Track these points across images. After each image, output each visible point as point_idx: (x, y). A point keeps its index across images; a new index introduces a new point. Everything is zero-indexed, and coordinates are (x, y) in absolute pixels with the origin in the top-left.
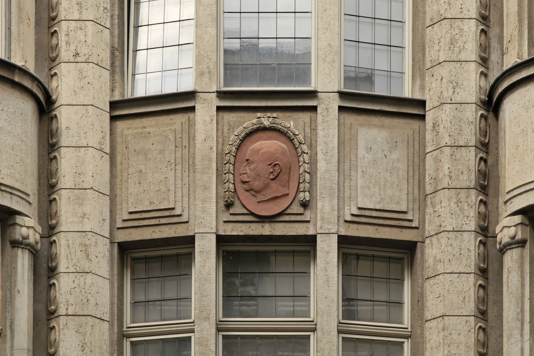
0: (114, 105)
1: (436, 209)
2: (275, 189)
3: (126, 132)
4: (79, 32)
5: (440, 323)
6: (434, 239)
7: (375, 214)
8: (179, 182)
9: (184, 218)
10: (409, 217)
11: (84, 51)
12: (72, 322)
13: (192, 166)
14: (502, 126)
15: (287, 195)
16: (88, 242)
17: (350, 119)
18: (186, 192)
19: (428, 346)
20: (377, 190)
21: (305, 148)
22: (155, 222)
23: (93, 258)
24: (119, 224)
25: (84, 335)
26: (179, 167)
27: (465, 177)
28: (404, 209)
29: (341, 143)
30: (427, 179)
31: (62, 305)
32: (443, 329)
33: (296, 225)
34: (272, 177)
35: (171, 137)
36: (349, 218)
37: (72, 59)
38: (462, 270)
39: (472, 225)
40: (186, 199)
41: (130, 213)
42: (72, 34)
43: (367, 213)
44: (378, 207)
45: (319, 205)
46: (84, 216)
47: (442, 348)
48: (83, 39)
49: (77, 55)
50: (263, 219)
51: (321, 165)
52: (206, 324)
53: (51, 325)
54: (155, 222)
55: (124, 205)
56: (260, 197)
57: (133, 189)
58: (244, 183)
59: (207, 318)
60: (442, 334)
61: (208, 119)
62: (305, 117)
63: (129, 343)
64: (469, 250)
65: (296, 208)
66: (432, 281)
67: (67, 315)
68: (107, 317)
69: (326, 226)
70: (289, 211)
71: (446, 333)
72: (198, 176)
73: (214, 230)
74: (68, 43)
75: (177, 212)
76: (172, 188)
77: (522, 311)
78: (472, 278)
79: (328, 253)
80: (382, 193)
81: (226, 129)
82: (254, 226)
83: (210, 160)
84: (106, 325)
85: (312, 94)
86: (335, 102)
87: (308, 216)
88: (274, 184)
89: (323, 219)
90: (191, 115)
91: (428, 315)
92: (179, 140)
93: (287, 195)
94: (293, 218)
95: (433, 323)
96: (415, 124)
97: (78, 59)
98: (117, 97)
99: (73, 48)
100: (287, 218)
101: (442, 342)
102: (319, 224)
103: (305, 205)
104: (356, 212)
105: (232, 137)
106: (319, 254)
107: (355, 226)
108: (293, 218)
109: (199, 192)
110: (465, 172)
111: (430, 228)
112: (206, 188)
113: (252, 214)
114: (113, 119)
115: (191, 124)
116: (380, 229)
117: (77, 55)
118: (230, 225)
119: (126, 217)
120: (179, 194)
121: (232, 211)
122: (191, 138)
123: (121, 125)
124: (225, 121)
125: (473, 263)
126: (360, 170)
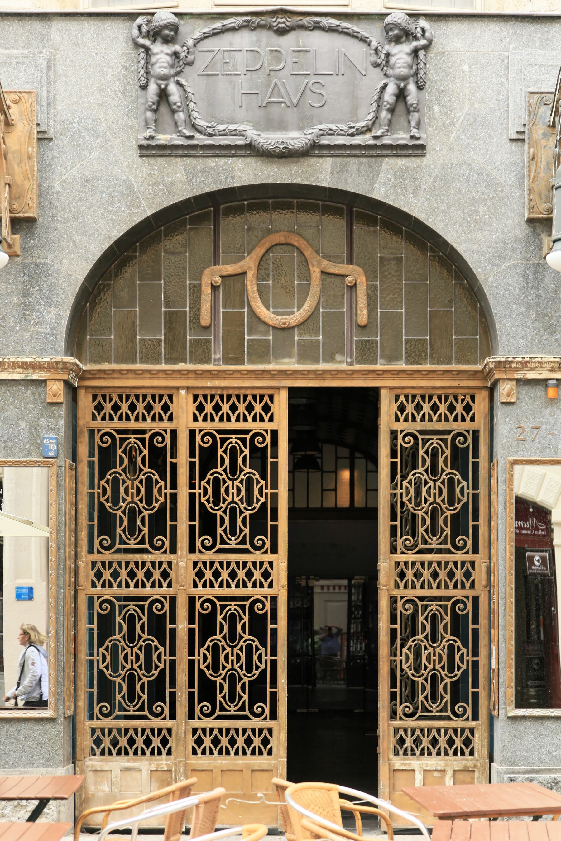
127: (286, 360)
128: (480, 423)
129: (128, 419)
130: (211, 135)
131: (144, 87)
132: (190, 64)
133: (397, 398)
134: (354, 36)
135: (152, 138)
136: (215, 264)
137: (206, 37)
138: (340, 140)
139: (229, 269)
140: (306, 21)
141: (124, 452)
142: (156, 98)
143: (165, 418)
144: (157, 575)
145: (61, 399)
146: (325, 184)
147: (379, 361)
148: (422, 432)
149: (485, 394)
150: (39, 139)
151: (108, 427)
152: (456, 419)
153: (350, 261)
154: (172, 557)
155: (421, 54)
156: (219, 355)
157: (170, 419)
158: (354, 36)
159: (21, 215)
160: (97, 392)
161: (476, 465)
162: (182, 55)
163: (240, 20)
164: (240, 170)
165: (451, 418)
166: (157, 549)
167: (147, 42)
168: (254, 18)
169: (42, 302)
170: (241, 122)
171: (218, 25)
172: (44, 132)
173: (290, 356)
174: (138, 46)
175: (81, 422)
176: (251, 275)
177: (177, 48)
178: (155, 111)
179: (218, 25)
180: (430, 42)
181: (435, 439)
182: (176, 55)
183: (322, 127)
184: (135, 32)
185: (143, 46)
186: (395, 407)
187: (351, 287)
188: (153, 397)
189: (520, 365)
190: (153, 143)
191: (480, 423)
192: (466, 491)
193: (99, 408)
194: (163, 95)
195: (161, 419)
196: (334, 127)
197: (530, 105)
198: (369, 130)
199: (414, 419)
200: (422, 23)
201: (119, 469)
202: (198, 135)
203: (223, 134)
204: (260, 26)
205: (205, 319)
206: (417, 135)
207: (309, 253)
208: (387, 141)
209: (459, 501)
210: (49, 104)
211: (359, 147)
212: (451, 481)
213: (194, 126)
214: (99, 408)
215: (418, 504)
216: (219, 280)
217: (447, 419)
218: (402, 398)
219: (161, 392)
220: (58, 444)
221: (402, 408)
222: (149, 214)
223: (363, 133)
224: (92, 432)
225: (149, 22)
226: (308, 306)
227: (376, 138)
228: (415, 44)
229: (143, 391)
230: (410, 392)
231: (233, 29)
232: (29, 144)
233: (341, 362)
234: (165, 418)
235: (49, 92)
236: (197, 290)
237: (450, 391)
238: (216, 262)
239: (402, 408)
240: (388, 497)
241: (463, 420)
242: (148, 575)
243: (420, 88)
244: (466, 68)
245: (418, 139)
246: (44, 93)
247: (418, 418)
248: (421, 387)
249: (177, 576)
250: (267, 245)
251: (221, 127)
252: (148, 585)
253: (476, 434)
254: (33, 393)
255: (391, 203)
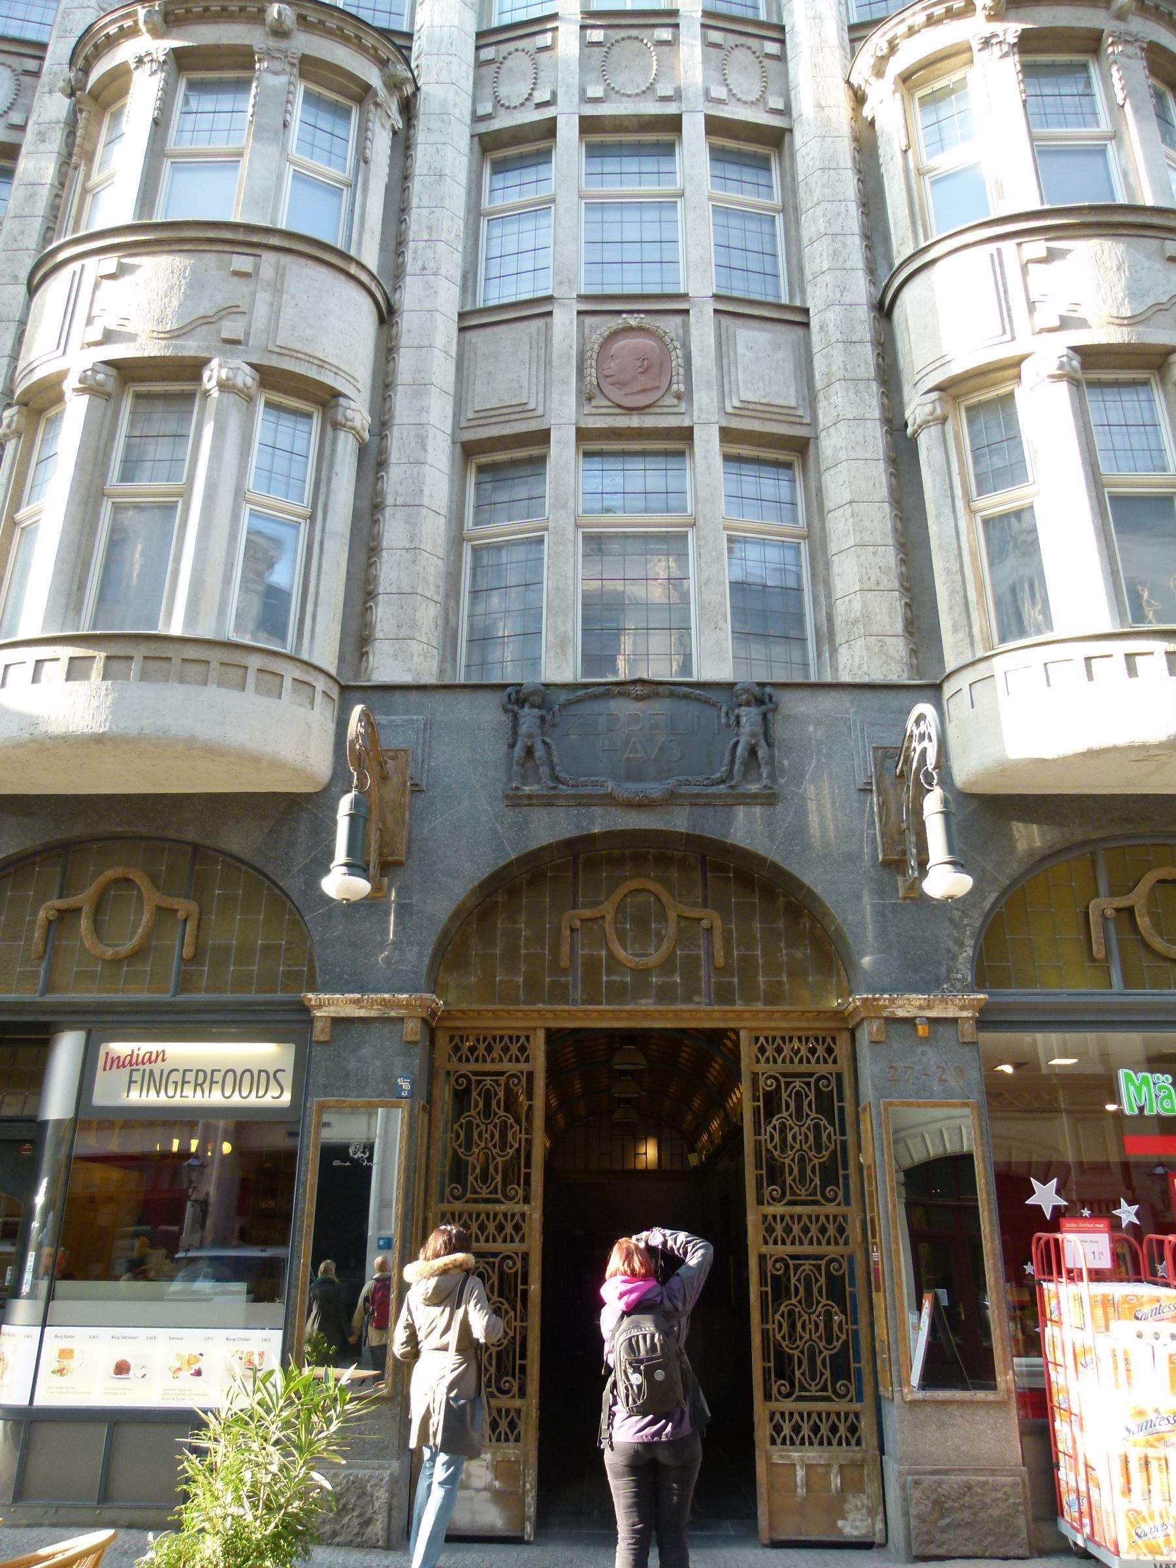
0: (462, 316)
1: (832, 400)
2: (644, 382)
3: (474, 340)
4: (427, 251)
5: (848, 510)
6: (832, 430)
7: (759, 408)
8: (534, 380)
9: (540, 412)
10: (800, 413)
11: (431, 265)
12: (401, 514)
13: (548, 363)
14: (902, 326)
15: (658, 388)
16: (424, 434)
17: (726, 321)
18: (541, 388)
19: (833, 537)
20: (761, 385)
21: (677, 344)
22: (507, 418)
23: (429, 448)
24: (464, 424)
25: (414, 525)
26: (534, 367)
27: (863, 369)
28: (793, 403)
29: (719, 343)
30: (817, 376)
31: (389, 496)
32: (853, 515)
33: (670, 417)
34: (640, 370)
35: (526, 339)
36: (729, 410)
37: (418, 272)
38: (869, 456)
39: (876, 413)
40: (541, 395)
41: (476, 412)
42: (419, 252)
43: (751, 406)
44: (764, 401)
45: (696, 396)
46: (422, 409)
47: (852, 535)
48: (432, 255)
49: (424, 268)
50: (630, 410)
51: (697, 361)
52: (563, 513)
53: (375, 518)
54: (507, 418)
55: (470, 405)
56: (626, 390)
57: (480, 388)
58: (607, 376)
59: (564, 507)
60: (850, 521)
61: (567, 321)
62: (678, 319)
63: (469, 548)
64: (874, 438)
65: (670, 400)
66: (832, 472)
67: (395, 505)
68: (443, 511)
69: (704, 416)
70: (660, 403)
71: (856, 519)
72: (555, 371)
73: (574, 421)
74: (415, 259)
75: (531, 406)
76: (526, 384)
77: (951, 487)
78: (881, 466)
79: (708, 441)
80: (767, 388)
81: (587, 331)
82: (619, 418)
83: (570, 358)
84: (442, 521)
85: (684, 297)
86: (711, 306)
87: (683, 408)
88: (642, 377)
89: (700, 409)
90: (548, 319)
91: (829, 505)
92: (534, 342)
93: (658, 388)
94: (666, 410)
95: (840, 512)
96: (800, 331)
97: (425, 272)
98: (468, 308)
99: (420, 263)
100: (659, 410)
101: (851, 529)
102: (696, 414)
103: (679, 397)
104: (737, 404)
105: (594, 336)
106: (696, 449)
107: (738, 419)
108: (666, 410)
109: (556, 389)
110: (862, 365)
111: (823, 420)
112: (564, 382)
113: (619, 406)
114: (462, 330)
115: (548, 328)
116: (766, 423)
117: (424, 268)
118: (592, 419)
119: (471, 415)
120: (534, 390)
121: (594, 403)
122: (548, 340)
123: (470, 335)
124: (587, 325)
125: (881, 450)
126: (740, 367)
127: (644, 1001)
128: (844, 1065)
129: (485, 1061)
130: (573, 786)
131: (512, 746)
132: (554, 726)
133: (757, 1039)
134: (706, 702)
135: (517, 788)
136: (574, 908)
137: (571, 703)
138: (696, 790)
139: (587, 913)
140: (661, 689)
141: (479, 1094)
142: (523, 754)
143: (522, 1059)
144: (509, 1229)
145: (418, 1038)
146: (683, 830)
147: (738, 1002)
148: (784, 1075)
149: (845, 1036)
150: (413, 791)
151: (465, 1068)
152: (818, 1062)
153: (705, 906)
154: (526, 1207)
155: (770, 716)
156: (578, 994)
157: (527, 1060)
158: (706, 702)
159: (390, 858)
160: (456, 1032)
161: (842, 1110)
162: (548, 718)
163: (602, 689)
164: (601, 817)
165: (813, 1061)
166: (510, 1199)
167: (516, 708)
168: (614, 688)
169: (405, 941)
170: (601, 775)
171: (581, 693)
172: (416, 785)
173: (648, 997)
174: (506, 711)
175: (437, 1064)
176: (609, 917)
177: (544, 712)
178: (522, 765)
179: (581, 693)
180: (777, 705)
181: (798, 1084)
182: (542, 719)
183: (680, 778)
184: (506, 699)
185: (512, 711)
186: (755, 1048)
187: (707, 930)
188: (511, 1038)
189: (887, 1003)
190: (520, 793)
191: (844, 1065)
192: (833, 1138)
193: (457, 1049)
194: (529, 752)
195: (518, 1060)
196: (690, 778)
197: (875, 759)
198: (723, 782)
199: (775, 1061)
200: (768, 690)
201: (473, 1112)
202: (561, 786)
203: (585, 785)
204: (620, 694)
205: (564, 962)
206: (769, 785)
207: (665, 897)
208: (741, 790)
209: (827, 1148)
210: (423, 761)
211: (715, 796)
212: (817, 1127)
213: (557, 779)
214: (457, 1049)
215: (783, 1151)
216: (578, 924)
217: (809, 1062)
218: (762, 1040)
219: (519, 1033)
220: (412, 1083)
221: (762, 1050)
222: (513, 857)
223: (718, 783)
224: (448, 1073)
225: (518, 692)
226: (665, 946)
227: (732, 787)
228: (763, 708)
229: (500, 1032)
230: (770, 1034)
231: (596, 697)
232: (403, 795)
233: (698, 1003)
234: (522, 1059)
235: (423, 751)
236: (557, 932)
237: (810, 1033)
238: (574, 907)
239: (762, 1050)
240: (752, 1144)
241: (826, 1062)
242: (500, 1228)
243: (770, 745)
244: (811, 728)
245: (771, 788)
246: (420, 751)
247: (780, 1060)
248: (782, 1029)
249: (530, 1229)
250: (626, 891)
251: (583, 779)
252: (499, 1239)
253: (839, 1077)
254: (391, 1031)
255: (747, 847)
